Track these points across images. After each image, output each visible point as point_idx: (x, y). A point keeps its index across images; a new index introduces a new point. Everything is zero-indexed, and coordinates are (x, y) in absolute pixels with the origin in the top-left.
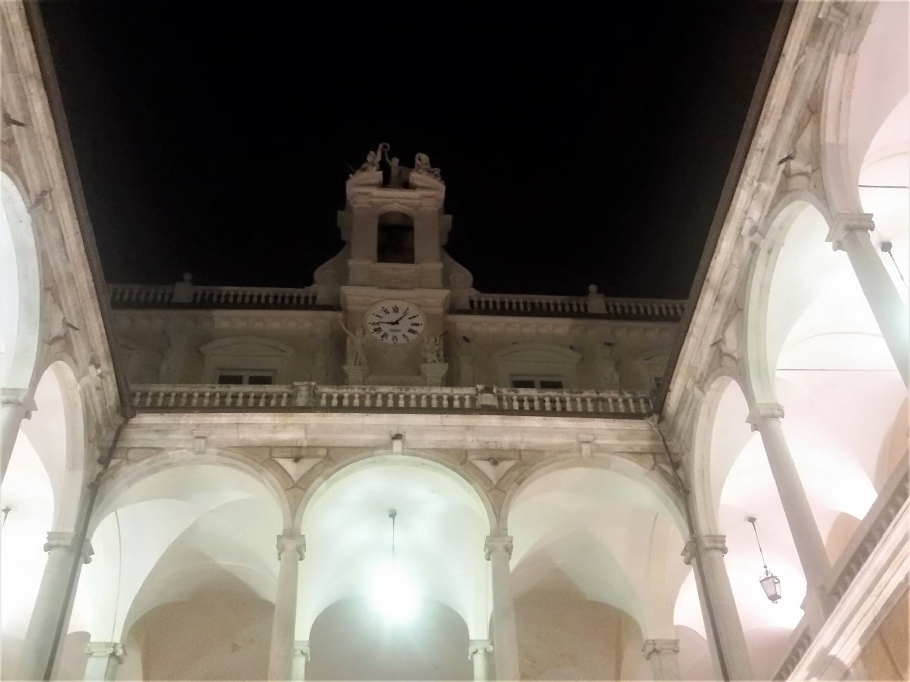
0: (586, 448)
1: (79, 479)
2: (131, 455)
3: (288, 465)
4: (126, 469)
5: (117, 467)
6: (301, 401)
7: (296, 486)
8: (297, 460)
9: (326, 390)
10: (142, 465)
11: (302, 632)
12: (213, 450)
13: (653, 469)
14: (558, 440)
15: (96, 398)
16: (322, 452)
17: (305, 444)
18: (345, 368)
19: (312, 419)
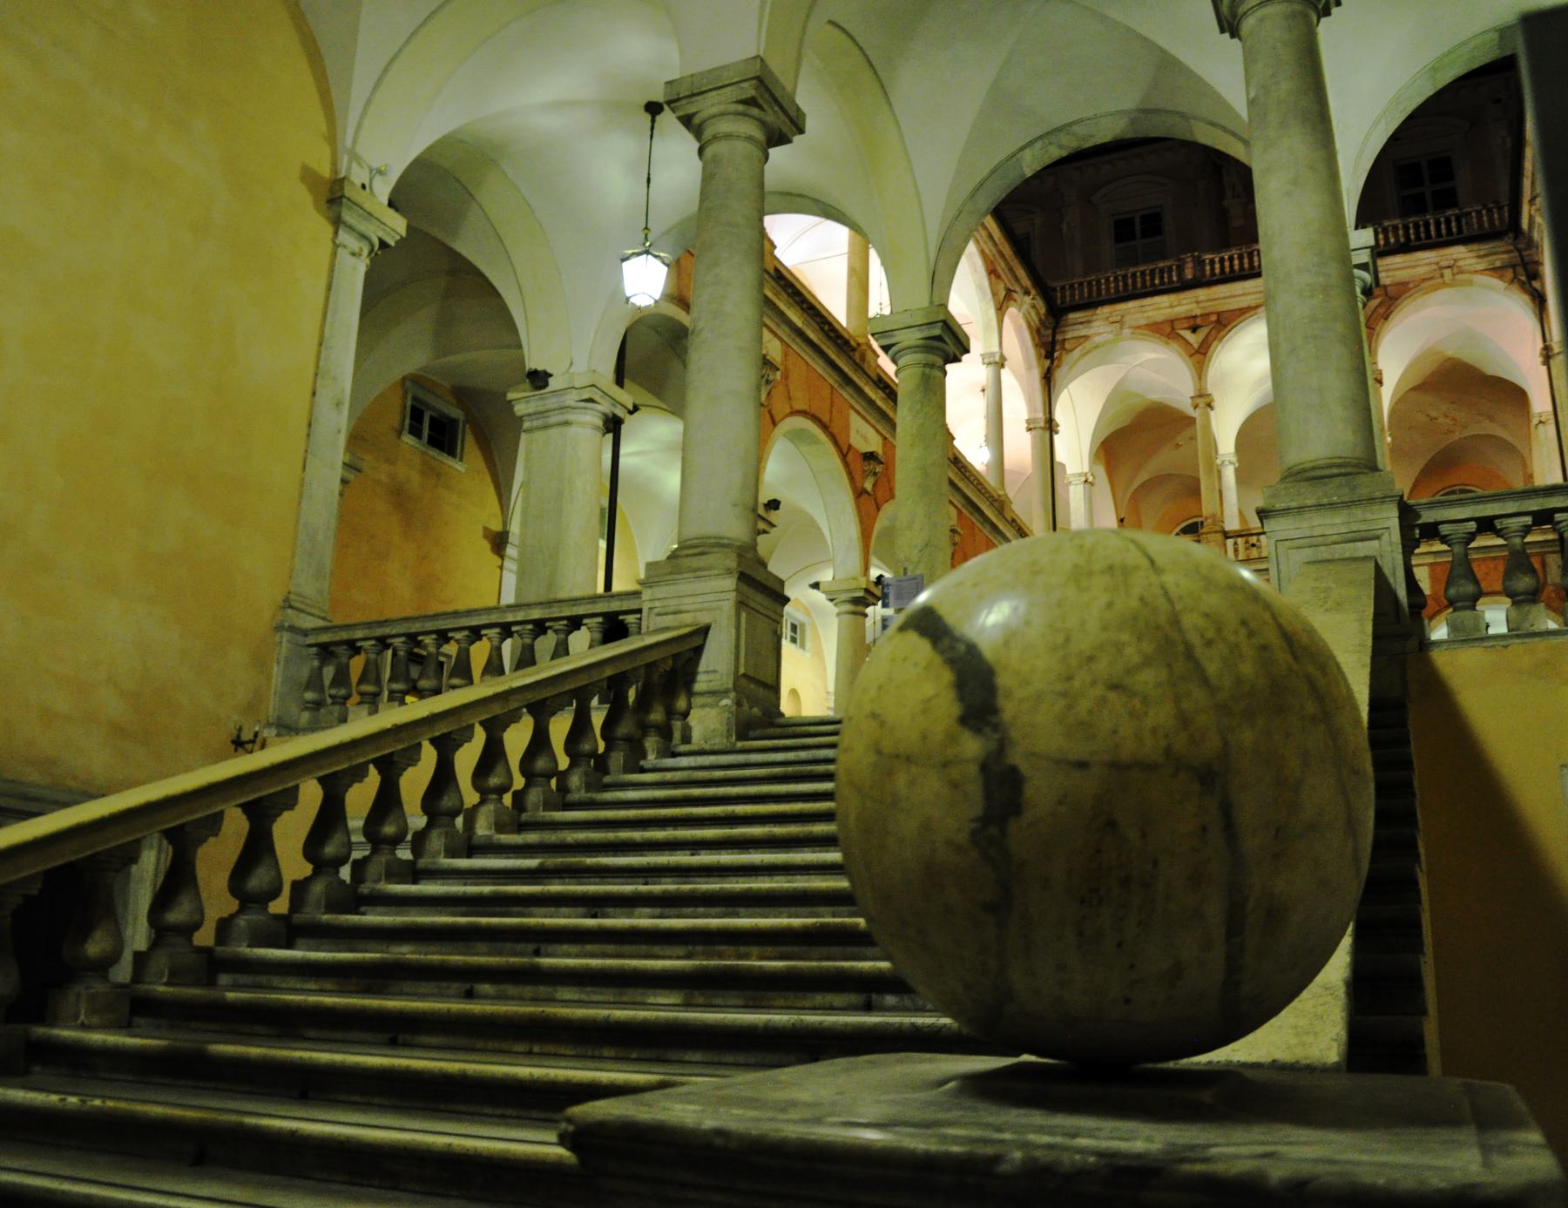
0: (1447, 272)
1: (1036, 374)
2: (1067, 346)
3: (1187, 334)
4: (1068, 359)
5: (1060, 358)
6: (1189, 274)
7: (1197, 352)
8: (1194, 330)
9: (1208, 257)
10: (1077, 352)
11: (1227, 445)
12: (1127, 331)
13: (1512, 282)
14: (1421, 271)
15: (1033, 314)
16: (1214, 318)
17: (1198, 312)
18: (1226, 203)
19: (1202, 293)
